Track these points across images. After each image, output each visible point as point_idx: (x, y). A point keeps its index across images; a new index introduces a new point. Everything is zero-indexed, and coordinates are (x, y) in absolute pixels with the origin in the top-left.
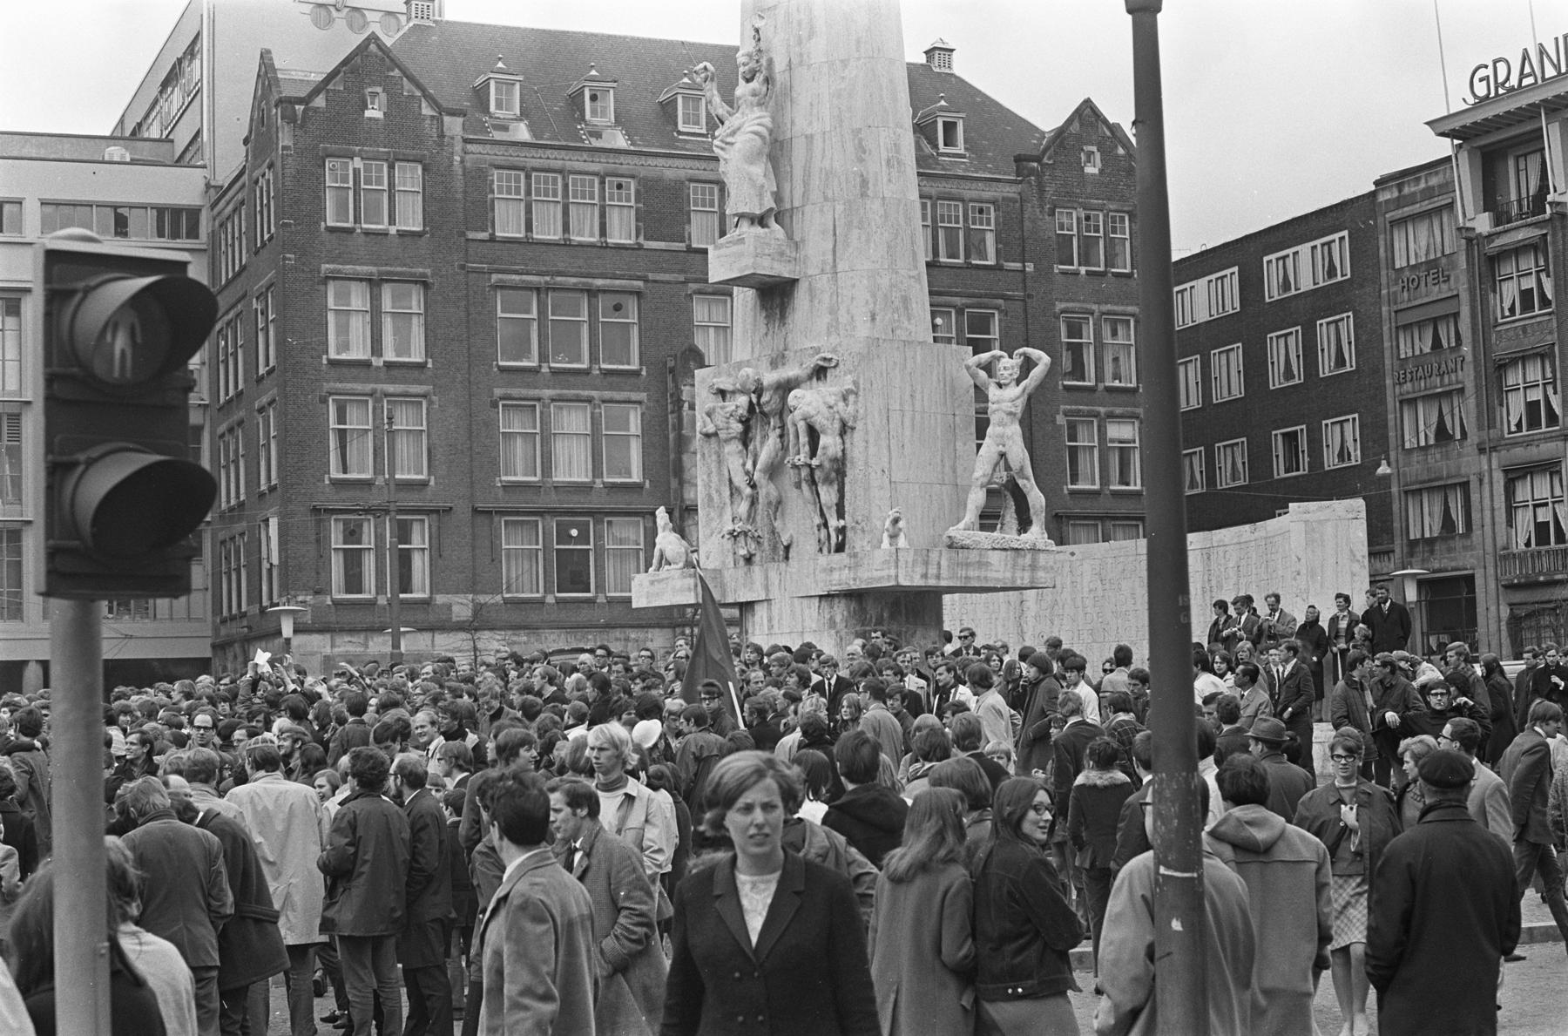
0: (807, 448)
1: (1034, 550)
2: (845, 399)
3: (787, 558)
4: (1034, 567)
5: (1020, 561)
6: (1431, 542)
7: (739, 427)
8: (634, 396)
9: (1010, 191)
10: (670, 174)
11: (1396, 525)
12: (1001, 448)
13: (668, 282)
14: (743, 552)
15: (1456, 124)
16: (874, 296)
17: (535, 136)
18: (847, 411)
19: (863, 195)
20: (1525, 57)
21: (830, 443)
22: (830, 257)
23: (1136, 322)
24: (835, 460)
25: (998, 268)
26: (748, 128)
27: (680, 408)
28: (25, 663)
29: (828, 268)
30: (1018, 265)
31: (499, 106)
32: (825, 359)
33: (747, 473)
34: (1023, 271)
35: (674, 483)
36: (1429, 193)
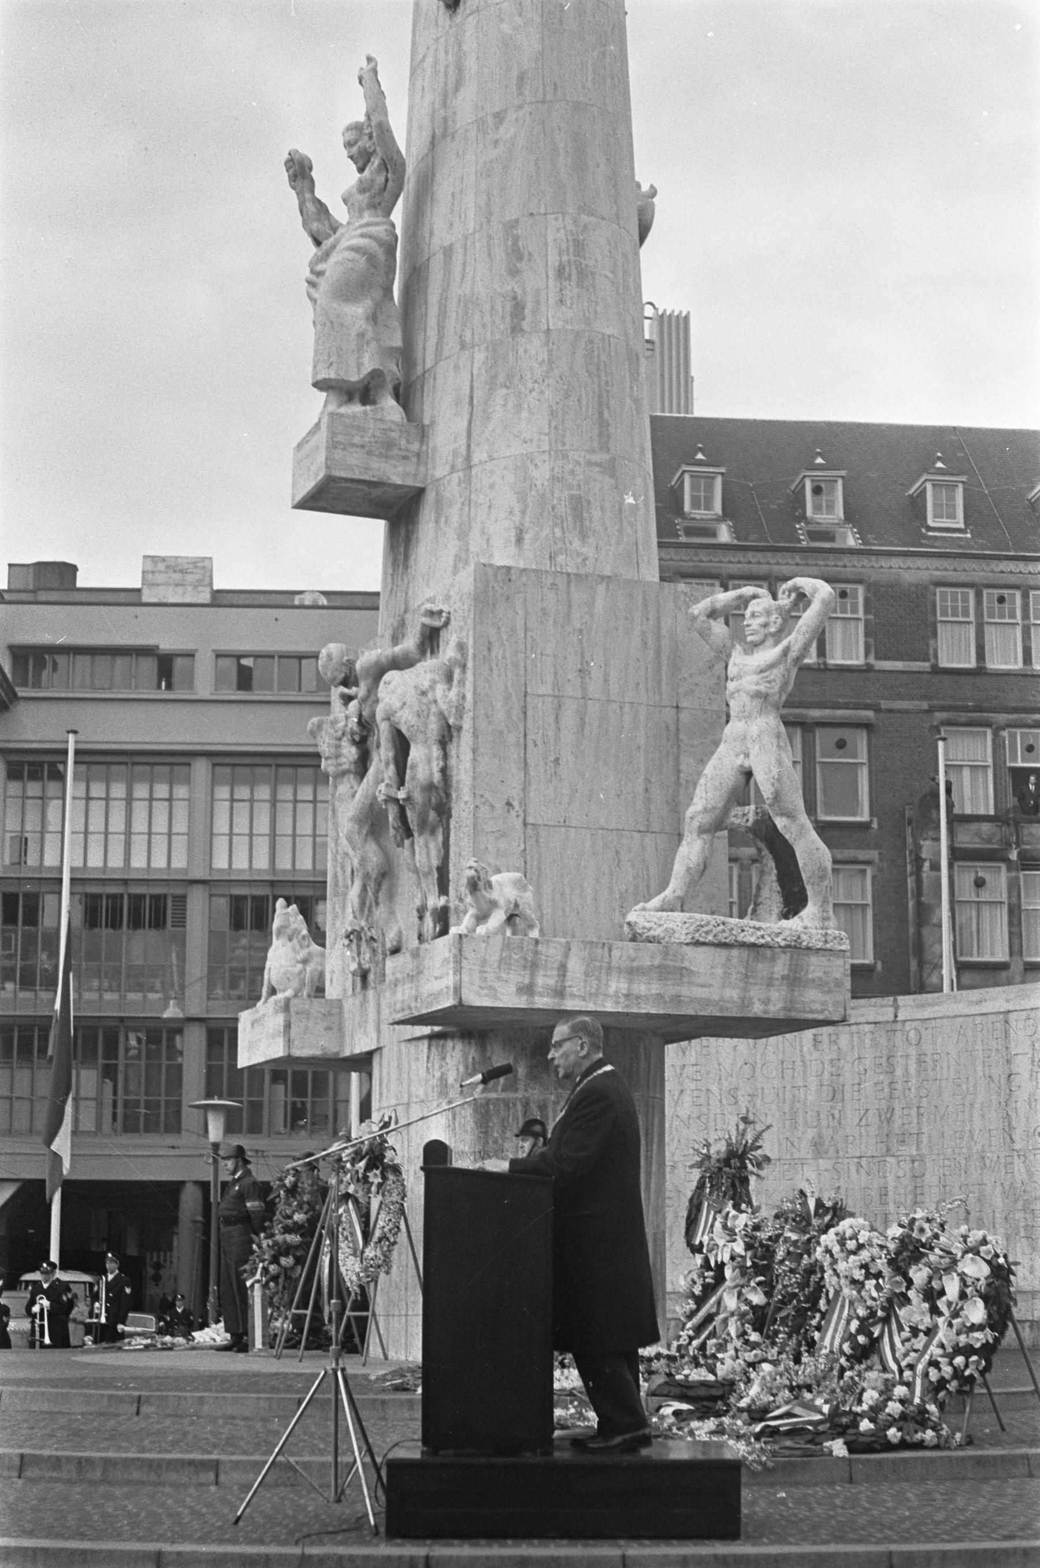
1: (796, 948)
2: (449, 678)
4: (794, 980)
5: (762, 969)
8: (862, 855)
10: (909, 577)
12: (740, 760)
13: (907, 711)
16: (522, 498)
17: (738, 538)
18: (445, 696)
19: (516, 330)
21: (423, 758)
22: (463, 441)
24: (430, 787)
26: (344, 243)
27: (919, 868)
28: (182, 1184)
31: (695, 503)
32: (431, 613)
35: (914, 965)
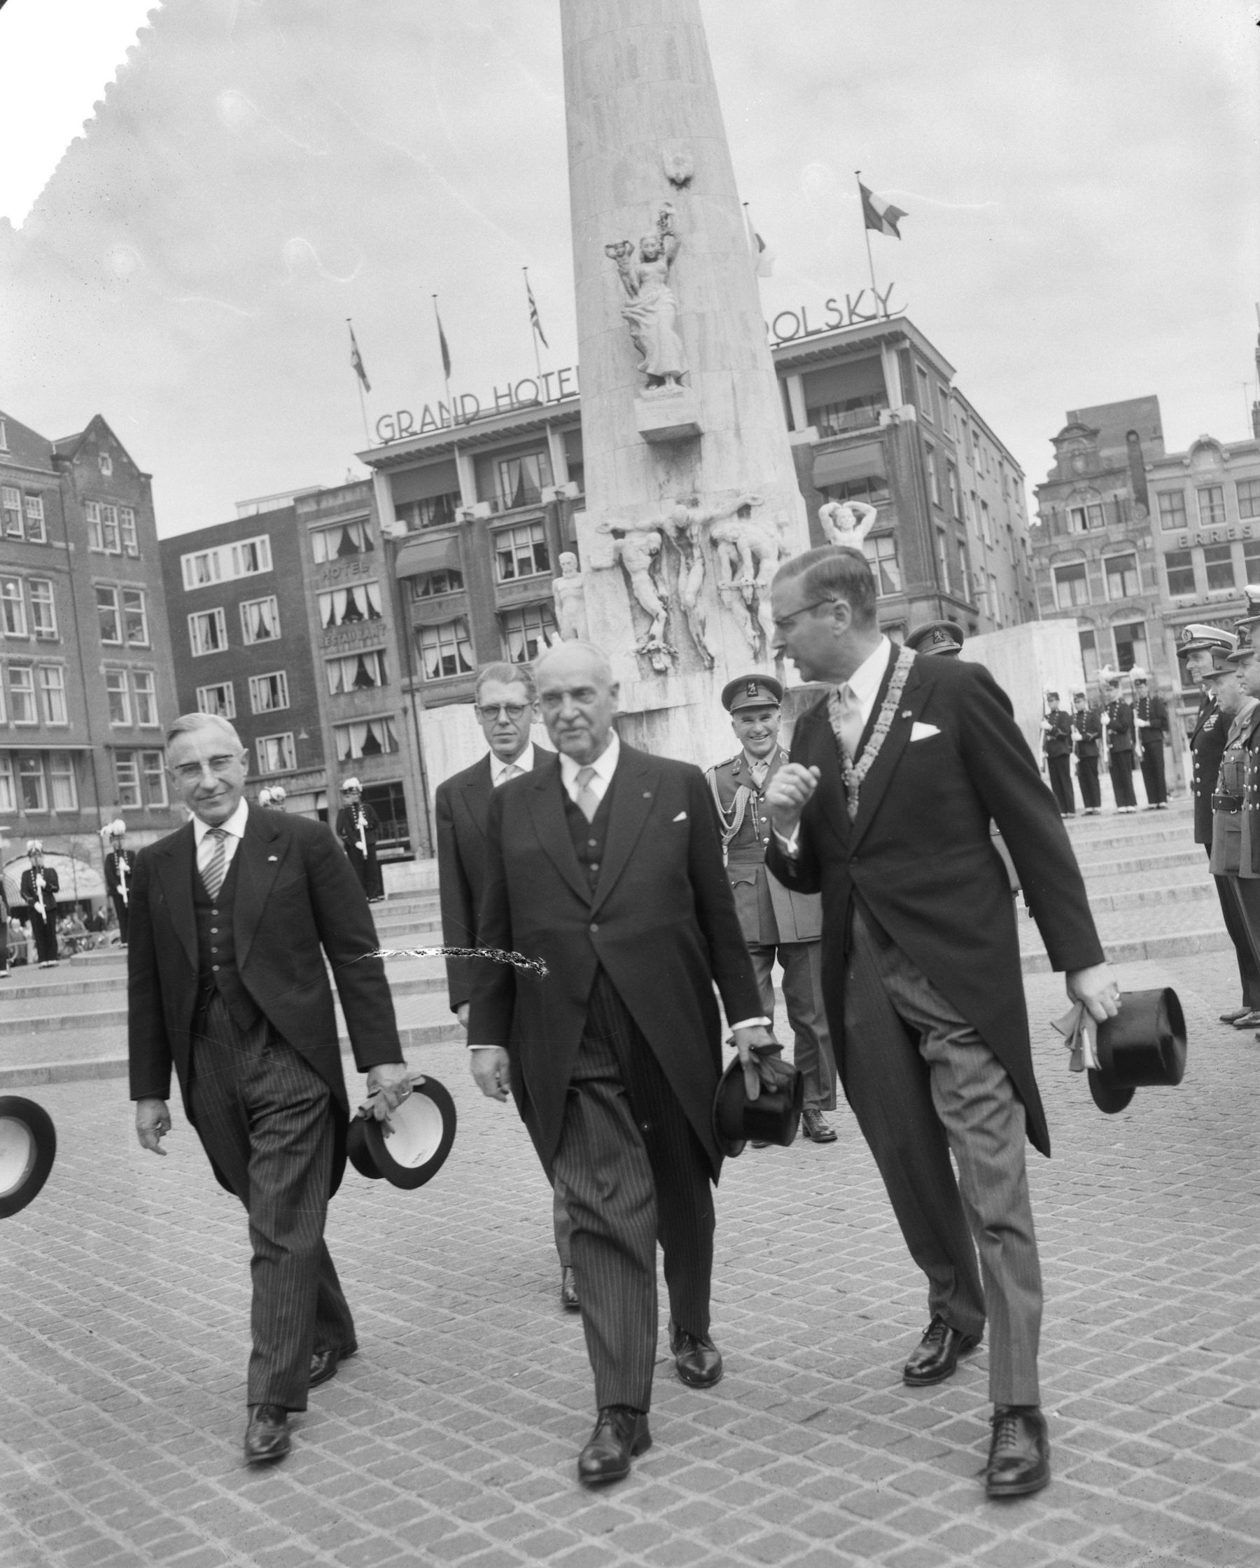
0: (752, 572)
3: (711, 668)
6: (359, 761)
7: (648, 560)
9: (53, 483)
11: (327, 751)
14: (658, 666)
15: (382, 456)
20: (426, 409)
23: (146, 595)
25: (48, 546)
29: (733, 425)
30: (62, 545)
32: (754, 499)
33: (661, 598)
34: (67, 550)
36: (347, 508)
